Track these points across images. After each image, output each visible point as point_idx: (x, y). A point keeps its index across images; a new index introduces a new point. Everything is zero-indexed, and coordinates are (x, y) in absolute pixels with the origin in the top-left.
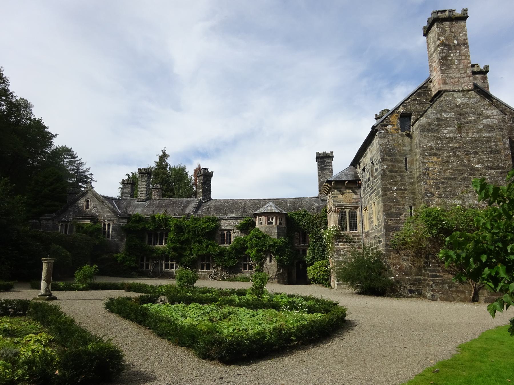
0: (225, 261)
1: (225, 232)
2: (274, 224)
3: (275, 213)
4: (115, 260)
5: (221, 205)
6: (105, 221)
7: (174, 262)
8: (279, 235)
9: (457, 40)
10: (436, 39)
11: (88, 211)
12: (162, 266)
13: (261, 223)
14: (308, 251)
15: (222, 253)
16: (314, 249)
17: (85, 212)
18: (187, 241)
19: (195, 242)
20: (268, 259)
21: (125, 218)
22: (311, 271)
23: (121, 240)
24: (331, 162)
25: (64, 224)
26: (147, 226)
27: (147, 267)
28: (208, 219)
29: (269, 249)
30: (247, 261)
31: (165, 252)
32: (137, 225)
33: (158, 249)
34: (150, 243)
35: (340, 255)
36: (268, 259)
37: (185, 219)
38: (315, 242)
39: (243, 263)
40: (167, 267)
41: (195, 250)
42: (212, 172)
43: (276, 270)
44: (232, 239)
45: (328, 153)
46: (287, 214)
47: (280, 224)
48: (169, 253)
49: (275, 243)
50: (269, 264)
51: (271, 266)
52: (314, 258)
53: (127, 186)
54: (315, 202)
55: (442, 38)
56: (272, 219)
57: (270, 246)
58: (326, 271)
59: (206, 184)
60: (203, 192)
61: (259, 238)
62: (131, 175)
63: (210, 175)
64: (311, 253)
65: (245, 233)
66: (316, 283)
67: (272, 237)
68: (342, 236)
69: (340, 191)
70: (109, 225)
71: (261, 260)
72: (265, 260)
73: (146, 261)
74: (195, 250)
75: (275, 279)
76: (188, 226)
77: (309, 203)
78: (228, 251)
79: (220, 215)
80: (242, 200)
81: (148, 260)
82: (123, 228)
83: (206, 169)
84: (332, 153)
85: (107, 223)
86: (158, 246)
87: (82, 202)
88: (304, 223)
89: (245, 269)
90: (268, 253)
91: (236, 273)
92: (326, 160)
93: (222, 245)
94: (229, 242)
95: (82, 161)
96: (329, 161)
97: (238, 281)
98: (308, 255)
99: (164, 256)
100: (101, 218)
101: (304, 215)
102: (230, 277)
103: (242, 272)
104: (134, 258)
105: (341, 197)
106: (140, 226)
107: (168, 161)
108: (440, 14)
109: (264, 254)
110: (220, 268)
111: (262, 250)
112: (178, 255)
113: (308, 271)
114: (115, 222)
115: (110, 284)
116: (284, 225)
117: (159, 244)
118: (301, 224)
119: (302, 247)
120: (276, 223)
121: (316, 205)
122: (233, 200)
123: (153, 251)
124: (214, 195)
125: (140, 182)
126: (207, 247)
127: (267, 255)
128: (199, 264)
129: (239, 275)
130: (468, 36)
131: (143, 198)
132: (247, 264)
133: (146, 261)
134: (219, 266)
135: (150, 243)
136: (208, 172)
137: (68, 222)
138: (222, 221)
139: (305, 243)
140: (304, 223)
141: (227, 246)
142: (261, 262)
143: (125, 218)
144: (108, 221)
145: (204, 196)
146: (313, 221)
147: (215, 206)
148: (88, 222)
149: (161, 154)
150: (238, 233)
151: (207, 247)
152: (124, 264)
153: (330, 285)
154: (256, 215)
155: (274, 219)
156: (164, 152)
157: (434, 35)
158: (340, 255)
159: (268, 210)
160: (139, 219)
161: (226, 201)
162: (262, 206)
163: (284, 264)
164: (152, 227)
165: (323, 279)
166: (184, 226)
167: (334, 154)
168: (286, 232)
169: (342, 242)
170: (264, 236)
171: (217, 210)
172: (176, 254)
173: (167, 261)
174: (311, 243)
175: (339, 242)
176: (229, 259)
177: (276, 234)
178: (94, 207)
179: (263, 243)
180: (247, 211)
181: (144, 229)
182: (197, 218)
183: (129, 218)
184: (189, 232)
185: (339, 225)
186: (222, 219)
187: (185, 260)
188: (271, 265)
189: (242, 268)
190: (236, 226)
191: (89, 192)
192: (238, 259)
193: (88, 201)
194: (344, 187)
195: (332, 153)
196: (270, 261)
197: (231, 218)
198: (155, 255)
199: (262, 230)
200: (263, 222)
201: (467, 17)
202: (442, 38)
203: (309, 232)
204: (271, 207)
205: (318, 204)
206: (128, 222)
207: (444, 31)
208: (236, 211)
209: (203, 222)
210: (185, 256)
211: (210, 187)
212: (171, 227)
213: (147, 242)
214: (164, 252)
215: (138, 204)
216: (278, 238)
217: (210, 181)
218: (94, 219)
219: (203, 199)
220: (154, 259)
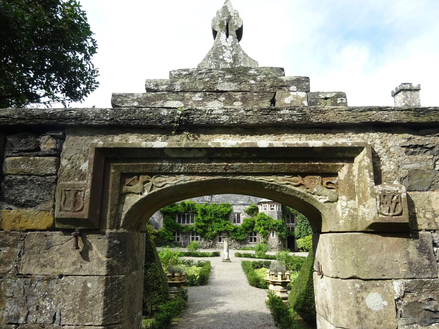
0: (238, 235)
1: (236, 215)
2: (275, 209)
7: (199, 237)
8: (278, 217)
9: (415, 103)
10: (402, 102)
12: (189, 239)
13: (266, 209)
18: (210, 221)
19: (215, 222)
20: (272, 234)
26: (179, 209)
27: (178, 239)
30: (252, 235)
31: (192, 229)
32: (171, 209)
34: (179, 221)
36: (272, 234)
38: (301, 222)
39: (249, 237)
40: (193, 239)
41: (216, 227)
48: (196, 229)
49: (278, 223)
51: (273, 239)
52: (300, 233)
55: (406, 102)
56: (274, 206)
57: (274, 225)
61: (265, 220)
66: (304, 251)
67: (274, 219)
71: (267, 235)
72: (270, 235)
73: (177, 235)
74: (216, 227)
76: (210, 210)
81: (178, 235)
89: (251, 241)
91: (245, 244)
93: (234, 224)
94: (239, 222)
99: (193, 232)
102: (241, 247)
103: (249, 244)
108: (404, 86)
109: (269, 231)
110: (233, 241)
111: (268, 228)
113: (298, 243)
116: (281, 211)
120: (276, 209)
123: (183, 228)
126: (225, 225)
128: (218, 238)
129: (247, 246)
130: (421, 101)
133: (177, 235)
134: (232, 239)
135: (179, 221)
138: (234, 207)
139: (293, 222)
141: (239, 225)
142: (266, 236)
151: (225, 225)
152: (165, 238)
155: (275, 206)
157: (400, 98)
164: (183, 211)
166: (207, 210)
172: (202, 230)
173: (193, 235)
174: (298, 223)
176: (241, 234)
177: (277, 217)
181: (177, 212)
184: (211, 214)
186: (233, 205)
187: (208, 235)
188: (274, 238)
189: (249, 241)
196: (273, 236)
197: (241, 205)
200: (267, 208)
201: (420, 90)
202: (406, 102)
207: (407, 97)
209: (221, 207)
213: (177, 222)
216: (278, 219)
220: (183, 234)
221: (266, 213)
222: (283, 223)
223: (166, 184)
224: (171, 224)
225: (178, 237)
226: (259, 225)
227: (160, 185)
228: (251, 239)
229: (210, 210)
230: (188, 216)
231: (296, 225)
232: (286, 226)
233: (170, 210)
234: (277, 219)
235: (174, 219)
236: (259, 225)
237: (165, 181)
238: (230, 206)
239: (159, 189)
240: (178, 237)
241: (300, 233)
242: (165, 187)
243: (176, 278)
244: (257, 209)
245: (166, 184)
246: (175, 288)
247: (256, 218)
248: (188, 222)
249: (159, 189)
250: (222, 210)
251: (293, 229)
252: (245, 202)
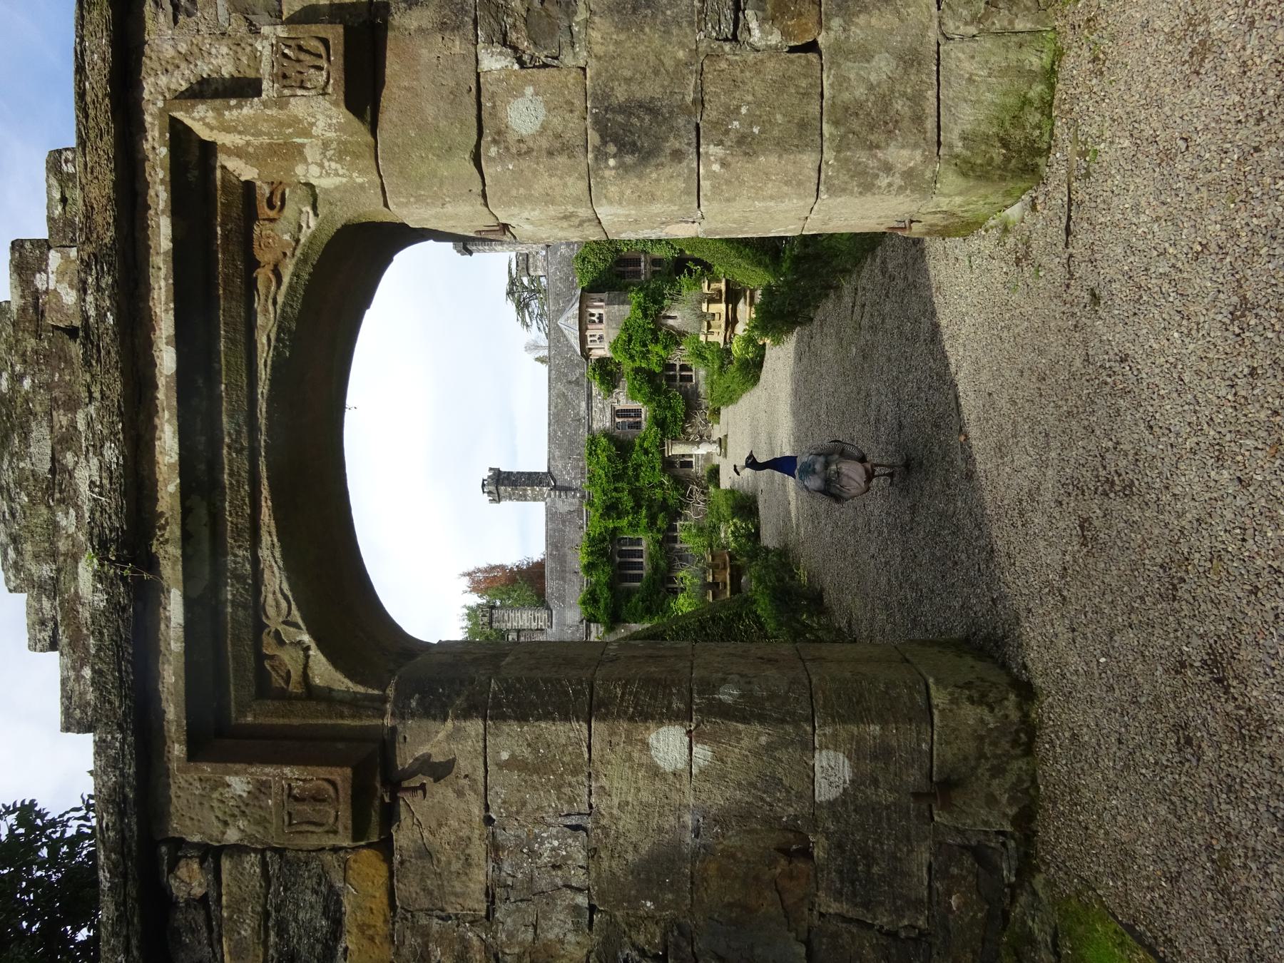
1: (618, 420)
2: (601, 311)
5: (560, 447)
8: (623, 303)
13: (601, 338)
18: (636, 494)
19: (637, 478)
20: (670, 322)
21: (588, 627)
26: (604, 579)
28: (590, 454)
31: (658, 541)
34: (638, 578)
36: (670, 322)
37: (591, 504)
39: (678, 383)
46: (583, 289)
47: (601, 301)
48: (659, 531)
49: (639, 304)
56: (593, 315)
57: (645, 316)
61: (630, 340)
67: (628, 314)
71: (672, 336)
72: (672, 327)
79: (583, 432)
83: (483, 485)
89: (690, 378)
91: (698, 396)
93: (644, 425)
94: (637, 413)
103: (697, 384)
106: (605, 594)
110: (690, 430)
116: (605, 296)
117: (640, 544)
118: (601, 266)
123: (656, 568)
124: (539, 465)
126: (646, 452)
131: (544, 614)
135: (638, 578)
138: (595, 426)
139: (638, 262)
141: (646, 412)
142: (675, 338)
143: (588, 627)
147: (562, 457)
151: (646, 452)
154: (585, 353)
155: (593, 311)
160: (591, 599)
164: (608, 569)
166: (604, 502)
172: (661, 516)
176: (670, 408)
177: (621, 307)
181: (611, 586)
182: (590, 479)
184: (616, 490)
186: (590, 428)
187: (673, 497)
189: (689, 385)
196: (674, 318)
200: (598, 333)
203: (618, 251)
206: (596, 621)
209: (598, 463)
210: (665, 499)
211: (523, 473)
215: (558, 624)
216: (629, 303)
217: (510, 474)
219: (548, 485)
220: (671, 568)
221: (613, 337)
222: (641, 290)
223: (281, 590)
224: (643, 601)
226: (644, 355)
227: (284, 604)
228: (683, 378)
230: (622, 554)
231: (645, 252)
232: (648, 281)
233: (606, 604)
235: (630, 593)
236: (644, 355)
237: (274, 593)
238: (594, 438)
239: (294, 606)
242: (289, 594)
243: (719, 579)
244: (602, 362)
245: (281, 590)
246: (744, 579)
247: (627, 366)
248: (639, 554)
249: (294, 606)
251: (656, 262)
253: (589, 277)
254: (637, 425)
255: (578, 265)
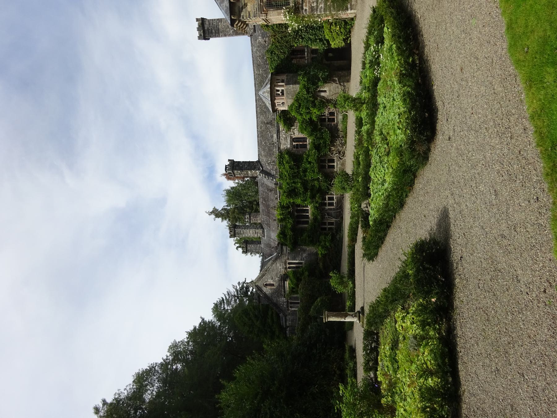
1: (294, 144)
2: (283, 88)
3: (271, 88)
4: (324, 256)
5: (264, 150)
6: (286, 268)
7: (327, 197)
8: (296, 83)
11: (276, 284)
12: (331, 209)
13: (283, 103)
14: (313, 48)
15: (317, 147)
16: (311, 40)
17: (278, 287)
18: (305, 184)
19: (305, 176)
20: (323, 94)
21: (282, 248)
22: (337, 43)
23: (304, 251)
24: (209, 21)
25: (290, 305)
26: (289, 226)
27: (332, 224)
28: (280, 163)
29: (312, 93)
32: (288, 236)
33: (313, 214)
34: (307, 223)
35: (317, 6)
36: (323, 94)
37: (281, 188)
38: (302, 38)
39: (327, 123)
40: (331, 204)
41: (313, 175)
42: (229, 160)
43: (334, 85)
44: (301, 135)
45: (199, 26)
46: (272, 74)
47: (283, 81)
48: (317, 202)
49: (304, 87)
50: (328, 93)
51: (330, 91)
52: (321, 40)
53: (249, 248)
54: (256, 40)
56: (278, 91)
57: (308, 92)
58: (336, 24)
59: (242, 167)
60: (251, 170)
61: (300, 106)
62: (238, 245)
63: (232, 162)
64: (315, 43)
65: (295, 122)
66: (350, 37)
67: (298, 90)
68: (295, 5)
69: (242, 8)
70: (289, 263)
71: (324, 103)
72: (323, 97)
74: (313, 175)
75: (344, 86)
76: (288, 184)
77: (259, 47)
78: (314, 140)
79: (276, 150)
80: (257, 126)
81: (325, 224)
82: (292, 250)
83: (226, 168)
84: (197, 20)
85: (288, 266)
86: (310, 214)
87: (267, 290)
88: (281, 52)
90: (315, 95)
91: (338, 130)
92: (206, 27)
93: (308, 147)
94: (304, 140)
95: (226, 293)
96: (207, 23)
97: (346, 127)
98: (317, 48)
99: (320, 208)
100: (283, 271)
101: (272, 53)
102: (343, 137)
103: (337, 124)
104: (322, 237)
105: (249, 7)
106: (289, 233)
107: (220, 208)
109: (317, 99)
110: (333, 148)
111: (313, 102)
112: (319, 193)
113: (336, 47)
114: (287, 258)
115: (349, 259)
116: (284, 77)
117: (308, 213)
118: (282, 56)
119: (309, 55)
120: (282, 86)
121: (260, 39)
122: (258, 136)
123: (315, 219)
124: (253, 157)
125: (244, 236)
126: (310, 163)
127: (318, 96)
128: (328, 170)
129: (340, 127)
131: (261, 231)
132: (328, 119)
134: (330, 149)
135: (307, 223)
136: (229, 165)
137: (287, 302)
138: (282, 147)
139: (302, 51)
140: (281, 52)
141: (309, 141)
142: (325, 102)
143: (282, 248)
144: (285, 264)
145: (255, 168)
146: (278, 42)
147: (265, 156)
148: (287, 283)
149: (213, 216)
150: (294, 129)
151: (310, 163)
152: (329, 247)
153: (352, 19)
154: (274, 110)
155: (278, 88)
156: (211, 213)
158: (317, 6)
159: (268, 96)
160: (283, 234)
161: (260, 144)
162: (264, 103)
163: (328, 75)
165: (345, 28)
166: (288, 188)
167: (199, 17)
168: (292, 75)
169: (302, 4)
170: (297, 100)
171: (269, 153)
174: (304, 44)
175: (302, 9)
176: (322, 138)
177: (294, 86)
178: (272, 279)
179: (305, 101)
180: (270, 120)
181: (293, 229)
182: (280, 175)
183: (281, 244)
184: (294, 182)
185: (282, 9)
186: (279, 148)
187: (324, 185)
188: (329, 90)
189: (333, 124)
190: (286, 132)
191: (257, 284)
192: (322, 129)
193: (266, 285)
194: (238, 4)
195: (197, 20)
196: (325, 91)
197: (278, 137)
198: (319, 217)
199: (290, 102)
200: (282, 101)
203: (291, 46)
204: (264, 93)
205: (259, 36)
206: (286, 245)
208: (270, 133)
209: (284, 168)
210: (320, 186)
212: (289, 202)
213: (307, 225)
214: (316, 208)
215: (267, 236)
216: (299, 83)
218: (284, 278)
219: (259, 169)
220: (323, 217)
225: (327, 224)
229: (288, 184)
230: (298, 211)
231: (308, 47)
234: (298, 86)
235: (303, 230)
240: (327, 224)
241: (321, 40)
248: (307, 211)
250: (287, 166)
251: (314, 51)
252: (274, 130)
253: (275, 64)
254: (305, 146)
255: (269, 55)
